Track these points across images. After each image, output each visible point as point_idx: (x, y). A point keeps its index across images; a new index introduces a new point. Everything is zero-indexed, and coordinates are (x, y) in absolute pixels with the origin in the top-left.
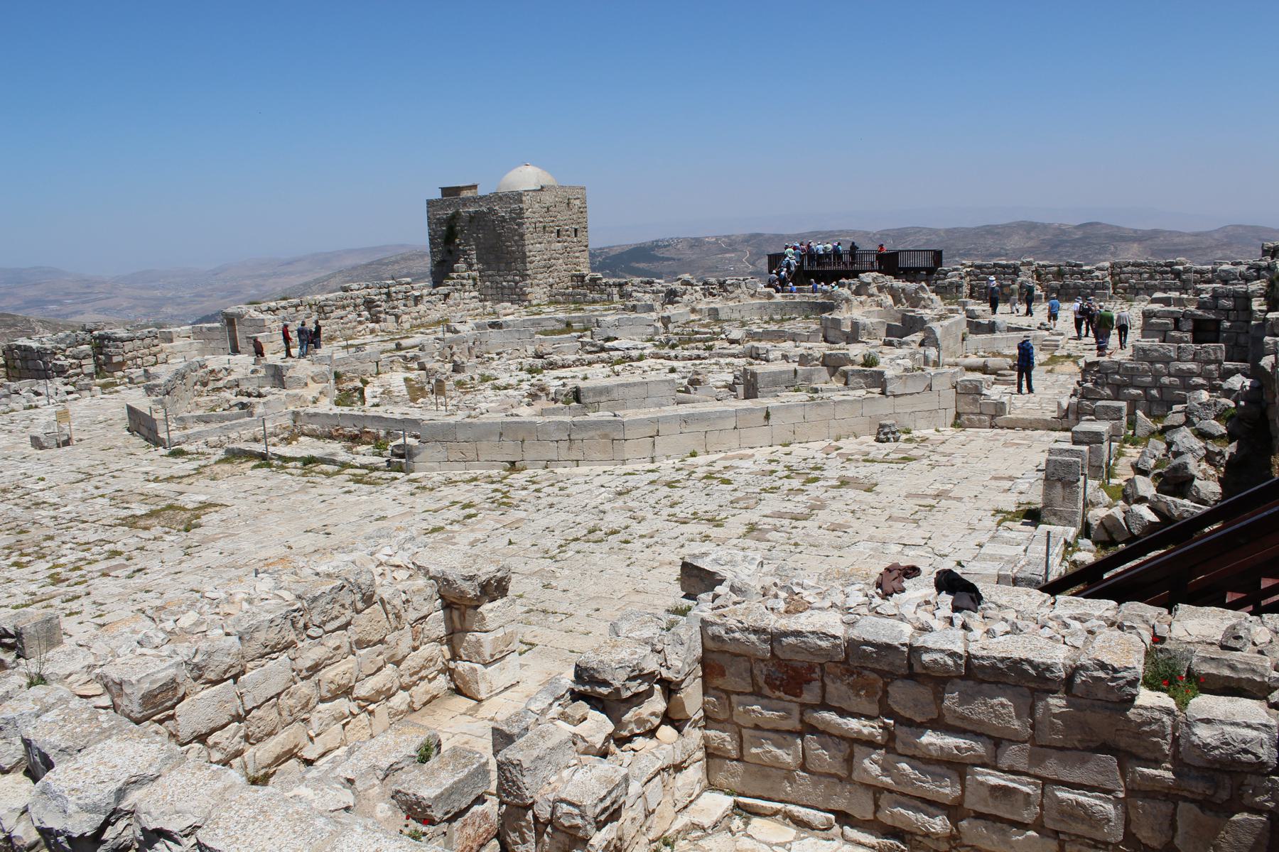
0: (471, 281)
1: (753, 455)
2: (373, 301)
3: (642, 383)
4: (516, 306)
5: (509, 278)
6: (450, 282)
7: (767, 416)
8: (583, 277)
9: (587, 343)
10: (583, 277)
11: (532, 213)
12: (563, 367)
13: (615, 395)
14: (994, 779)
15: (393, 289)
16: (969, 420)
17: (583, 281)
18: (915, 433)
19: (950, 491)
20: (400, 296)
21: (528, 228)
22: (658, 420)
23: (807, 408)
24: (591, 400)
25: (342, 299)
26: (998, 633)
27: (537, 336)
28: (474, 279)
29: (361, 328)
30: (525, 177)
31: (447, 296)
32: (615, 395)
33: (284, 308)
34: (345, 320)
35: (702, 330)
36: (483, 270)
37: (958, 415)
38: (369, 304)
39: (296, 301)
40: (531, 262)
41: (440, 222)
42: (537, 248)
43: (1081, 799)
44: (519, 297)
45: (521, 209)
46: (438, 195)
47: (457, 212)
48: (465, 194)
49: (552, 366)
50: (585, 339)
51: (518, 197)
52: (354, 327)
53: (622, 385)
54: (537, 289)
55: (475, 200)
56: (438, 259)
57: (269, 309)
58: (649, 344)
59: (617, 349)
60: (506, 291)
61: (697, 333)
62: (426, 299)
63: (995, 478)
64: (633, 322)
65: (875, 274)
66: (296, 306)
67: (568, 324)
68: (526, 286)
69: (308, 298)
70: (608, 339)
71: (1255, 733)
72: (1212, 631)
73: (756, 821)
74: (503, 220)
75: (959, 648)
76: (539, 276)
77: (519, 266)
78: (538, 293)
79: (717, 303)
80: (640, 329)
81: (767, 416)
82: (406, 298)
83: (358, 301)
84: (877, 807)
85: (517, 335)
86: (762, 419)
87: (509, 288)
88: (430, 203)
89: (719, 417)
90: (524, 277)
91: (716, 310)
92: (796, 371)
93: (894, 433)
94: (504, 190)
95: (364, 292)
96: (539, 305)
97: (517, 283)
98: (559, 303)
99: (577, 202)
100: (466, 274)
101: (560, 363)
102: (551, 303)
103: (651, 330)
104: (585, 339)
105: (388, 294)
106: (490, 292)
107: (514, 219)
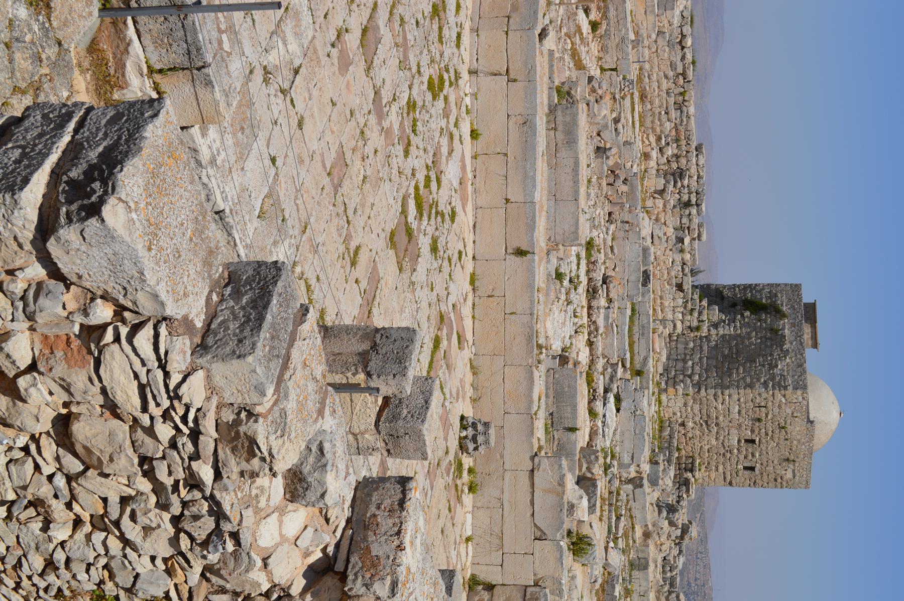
0: (695, 323)
2: (681, 177)
3: (577, 192)
4: (660, 370)
5: (697, 369)
6: (696, 297)
7: (520, 253)
8: (691, 471)
9: (615, 371)
10: (691, 471)
11: (779, 403)
12: (590, 307)
13: (564, 153)
15: (694, 211)
17: (686, 470)
18: (468, 499)
20: (685, 220)
21: (760, 394)
22: (531, 79)
23: (526, 319)
24: (560, 119)
25: (688, 138)
27: (629, 306)
28: (698, 328)
29: (653, 139)
30: (825, 408)
31: (680, 287)
32: (564, 153)
33: (683, 58)
34: (664, 117)
35: (622, 525)
36: (709, 341)
37: (490, 587)
38: (680, 174)
39: (690, 74)
40: (715, 395)
41: (773, 296)
42: (733, 404)
44: (672, 377)
45: (785, 388)
46: (807, 298)
47: (784, 316)
48: (807, 329)
49: (592, 292)
50: (620, 370)
51: (801, 386)
52: (654, 130)
53: (577, 163)
54: (680, 404)
55: (799, 336)
56: (725, 292)
57: (683, 36)
58: (608, 444)
60: (680, 365)
61: (618, 518)
62: (678, 257)
64: (638, 434)
66: (684, 74)
67: (639, 373)
68: (685, 385)
69: (692, 95)
74: (773, 366)
76: (697, 407)
77: (712, 381)
78: (676, 403)
79: (654, 573)
80: (628, 444)
81: (520, 253)
82: (681, 228)
83: (683, 161)
85: (633, 278)
86: (514, 244)
87: (684, 369)
88: (796, 288)
89: (525, 176)
90: (698, 386)
91: (646, 567)
92: (573, 430)
93: (474, 439)
94: (810, 380)
95: (693, 170)
96: (660, 403)
97: (690, 376)
98: (661, 431)
99: (789, 475)
100: (705, 317)
101: (594, 303)
102: (662, 422)
103: (626, 459)
104: (620, 370)
105: (688, 204)
106: (681, 347)
107: (773, 378)
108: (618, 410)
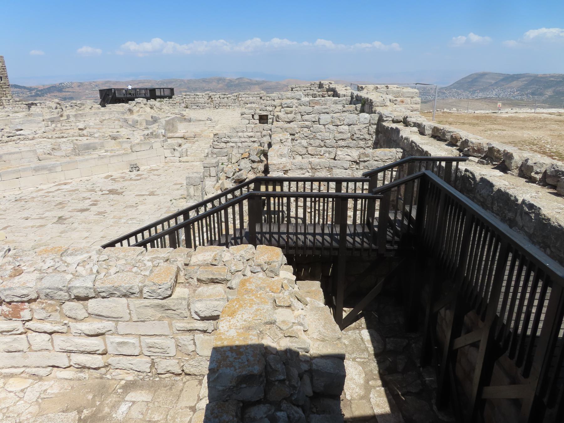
1: (71, 182)
3: (17, 153)
14: (119, 339)
16: (170, 159)
19: (155, 191)
26: (112, 274)
43: (156, 341)
59: (23, 135)
63: (175, 184)
65: (141, 99)
70: (17, 130)
71: (219, 302)
72: (209, 257)
73: (11, 381)
75: (90, 285)
84: (70, 360)
108: (22, 130)
